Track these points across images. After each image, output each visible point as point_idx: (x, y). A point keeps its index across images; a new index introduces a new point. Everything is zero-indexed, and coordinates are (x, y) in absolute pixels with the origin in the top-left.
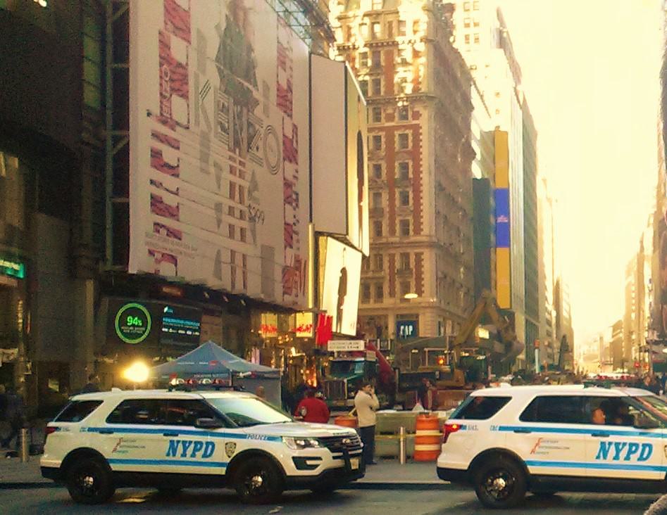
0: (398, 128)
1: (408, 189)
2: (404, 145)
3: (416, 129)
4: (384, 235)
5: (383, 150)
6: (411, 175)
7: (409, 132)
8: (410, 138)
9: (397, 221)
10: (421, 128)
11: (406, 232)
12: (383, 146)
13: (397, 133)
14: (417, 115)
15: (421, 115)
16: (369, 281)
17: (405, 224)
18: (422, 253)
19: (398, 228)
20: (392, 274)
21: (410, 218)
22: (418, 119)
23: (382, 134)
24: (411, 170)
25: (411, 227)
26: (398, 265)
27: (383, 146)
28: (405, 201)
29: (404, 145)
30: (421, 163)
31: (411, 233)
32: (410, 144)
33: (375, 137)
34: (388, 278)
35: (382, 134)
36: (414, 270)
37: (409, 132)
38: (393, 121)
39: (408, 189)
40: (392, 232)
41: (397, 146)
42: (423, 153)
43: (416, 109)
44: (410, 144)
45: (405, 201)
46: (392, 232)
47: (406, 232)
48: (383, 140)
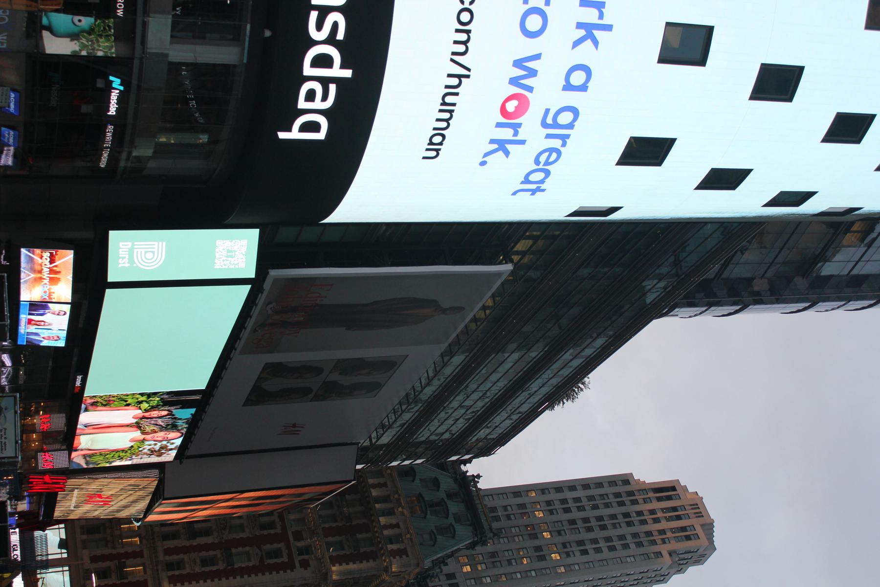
1: (220, 563)
2: (270, 555)
3: (289, 566)
4: (165, 542)
5: (262, 532)
7: (285, 559)
8: (279, 561)
9: (181, 556)
10: (292, 571)
11: (170, 566)
12: (265, 532)
13: (282, 545)
14: (305, 565)
15: (306, 569)
17: (179, 565)
21: (188, 570)
22: (301, 567)
23: (279, 530)
25: (177, 573)
27: (265, 532)
28: (205, 562)
29: (270, 555)
30: (253, 575)
31: (170, 573)
32: (272, 561)
33: (273, 522)
34: (114, 552)
35: (279, 530)
36: (126, 581)
37: (285, 559)
38: (295, 540)
39: (220, 563)
40: (168, 552)
41: (268, 547)
42: (264, 576)
43: (311, 562)
44: (272, 561)
45: (205, 562)
46: (168, 552)
47: (170, 566)
48: (272, 532)
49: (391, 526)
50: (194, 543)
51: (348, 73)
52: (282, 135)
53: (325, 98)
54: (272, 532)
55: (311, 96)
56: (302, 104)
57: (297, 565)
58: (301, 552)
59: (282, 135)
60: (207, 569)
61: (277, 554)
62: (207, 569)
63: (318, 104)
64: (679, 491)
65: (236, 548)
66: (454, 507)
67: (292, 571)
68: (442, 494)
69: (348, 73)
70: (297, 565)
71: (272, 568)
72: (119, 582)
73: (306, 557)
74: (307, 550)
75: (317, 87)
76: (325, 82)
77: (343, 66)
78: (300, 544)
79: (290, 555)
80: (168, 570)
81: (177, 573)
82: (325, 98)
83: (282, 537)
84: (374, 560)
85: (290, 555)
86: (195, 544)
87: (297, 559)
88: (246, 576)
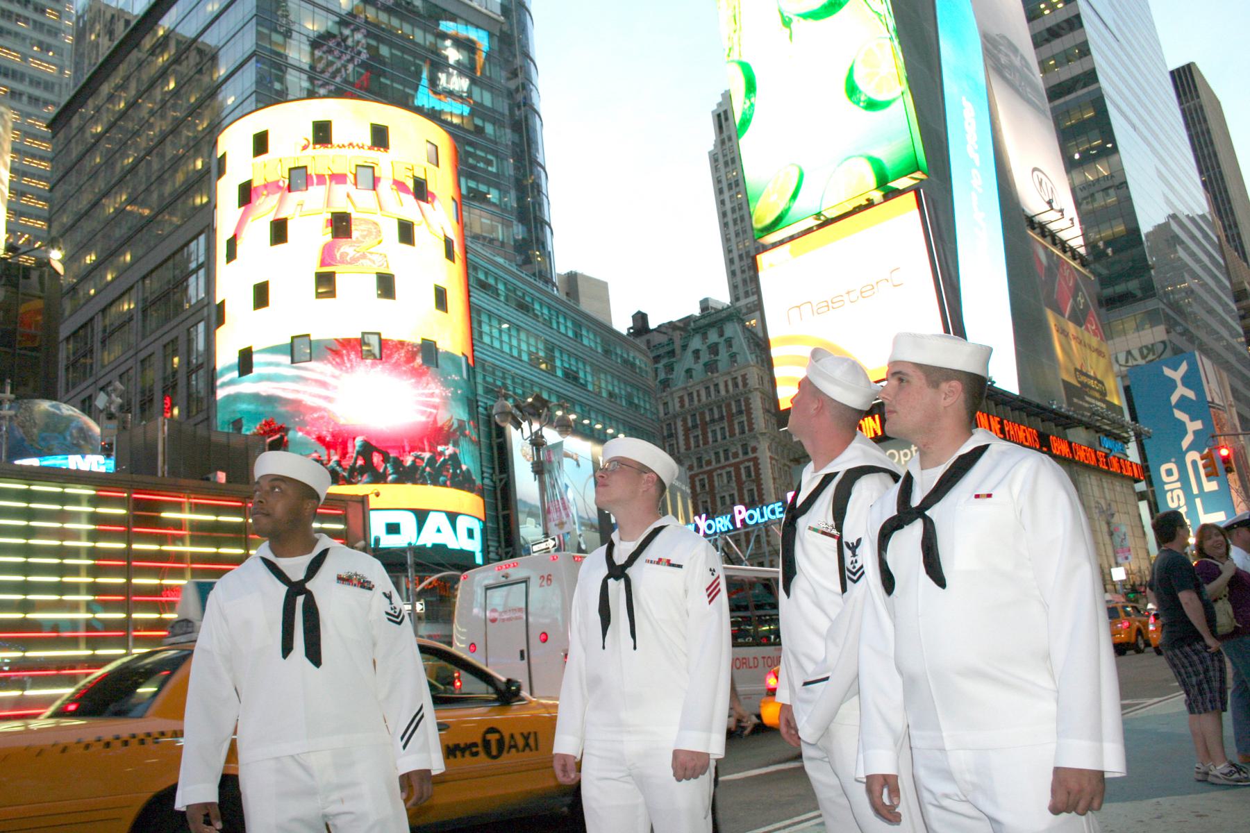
3: (755, 460)
8: (752, 469)
12: (734, 478)
13: (742, 467)
14: (754, 450)
24: (756, 494)
29: (749, 475)
44: (753, 474)
48: (733, 474)
49: (726, 386)
58: (746, 453)
61: (748, 468)
64: (721, 111)
66: (713, 337)
68: (704, 348)
71: (758, 474)
74: (744, 447)
78: (740, 453)
79: (749, 460)
83: (737, 466)
85: (749, 460)
87: (751, 455)
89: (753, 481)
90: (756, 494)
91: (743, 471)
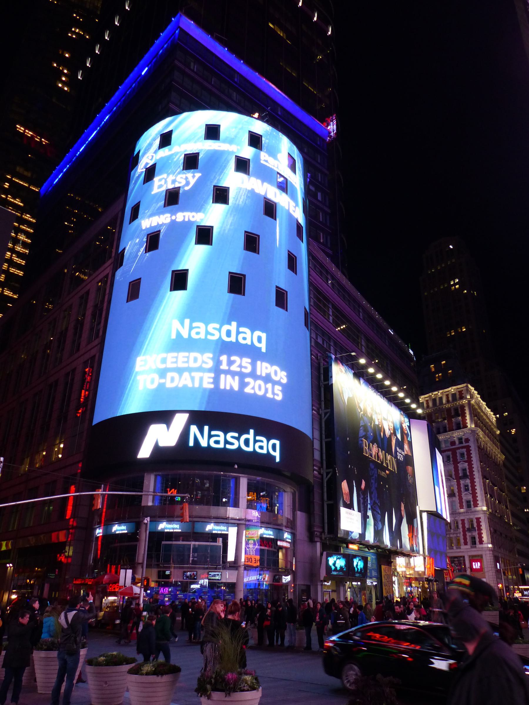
0: (459, 448)
1: (467, 481)
3: (468, 448)
6: (468, 474)
7: (464, 450)
8: (465, 453)
10: (470, 447)
12: (451, 459)
13: (458, 451)
16: (451, 536)
17: (468, 502)
18: (480, 518)
19: (464, 504)
20: (464, 531)
24: (468, 470)
25: (472, 503)
26: (467, 526)
28: (467, 490)
30: (473, 466)
31: (472, 506)
32: (466, 456)
34: (462, 533)
36: (476, 528)
37: (464, 450)
47: (469, 506)
50: (457, 494)
51: (252, 431)
52: (278, 460)
53: (262, 441)
54: (451, 456)
55: (261, 447)
56: (264, 451)
57: (467, 444)
58: (461, 442)
59: (278, 460)
60: (470, 488)
61: (462, 455)
62: (470, 488)
63: (264, 444)
65: (459, 474)
67: (470, 447)
69: (252, 431)
70: (467, 444)
72: (477, 532)
73: (463, 440)
75: (258, 444)
76: (255, 441)
77: (248, 433)
78: (457, 442)
79: (463, 447)
80: (471, 507)
81: (472, 503)
82: (262, 441)
83: (454, 451)
84: (465, 407)
85: (463, 447)
86: (458, 494)
87: (464, 444)
88: (473, 469)
89: (465, 462)
90: (468, 470)
91: (458, 455)
